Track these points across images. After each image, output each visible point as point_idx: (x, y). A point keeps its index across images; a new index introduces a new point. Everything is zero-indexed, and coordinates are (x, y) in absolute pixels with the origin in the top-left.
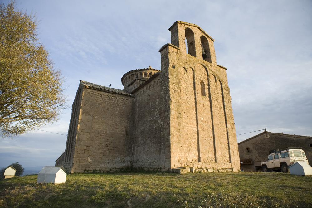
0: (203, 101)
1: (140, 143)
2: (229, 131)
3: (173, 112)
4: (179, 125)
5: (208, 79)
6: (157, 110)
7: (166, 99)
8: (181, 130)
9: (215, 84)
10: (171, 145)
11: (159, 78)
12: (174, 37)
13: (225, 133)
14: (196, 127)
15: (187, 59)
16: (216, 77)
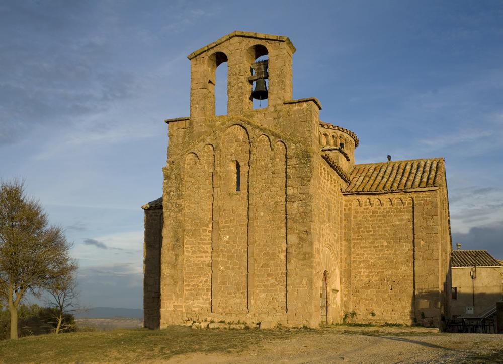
2: (290, 250)
4: (176, 259)
8: (178, 266)
9: (272, 153)
10: (161, 290)
13: (282, 256)
15: (207, 129)
16: (272, 138)
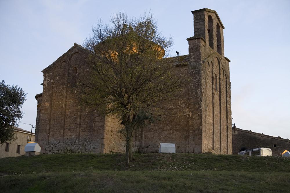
0: (216, 96)
1: (153, 129)
3: (203, 106)
5: (220, 73)
6: (181, 99)
7: (196, 93)
11: (186, 68)
12: (198, 24)
13: (226, 127)
14: (212, 119)
